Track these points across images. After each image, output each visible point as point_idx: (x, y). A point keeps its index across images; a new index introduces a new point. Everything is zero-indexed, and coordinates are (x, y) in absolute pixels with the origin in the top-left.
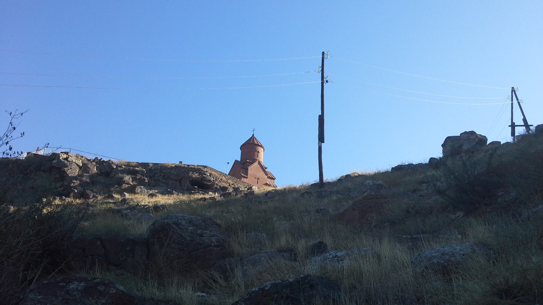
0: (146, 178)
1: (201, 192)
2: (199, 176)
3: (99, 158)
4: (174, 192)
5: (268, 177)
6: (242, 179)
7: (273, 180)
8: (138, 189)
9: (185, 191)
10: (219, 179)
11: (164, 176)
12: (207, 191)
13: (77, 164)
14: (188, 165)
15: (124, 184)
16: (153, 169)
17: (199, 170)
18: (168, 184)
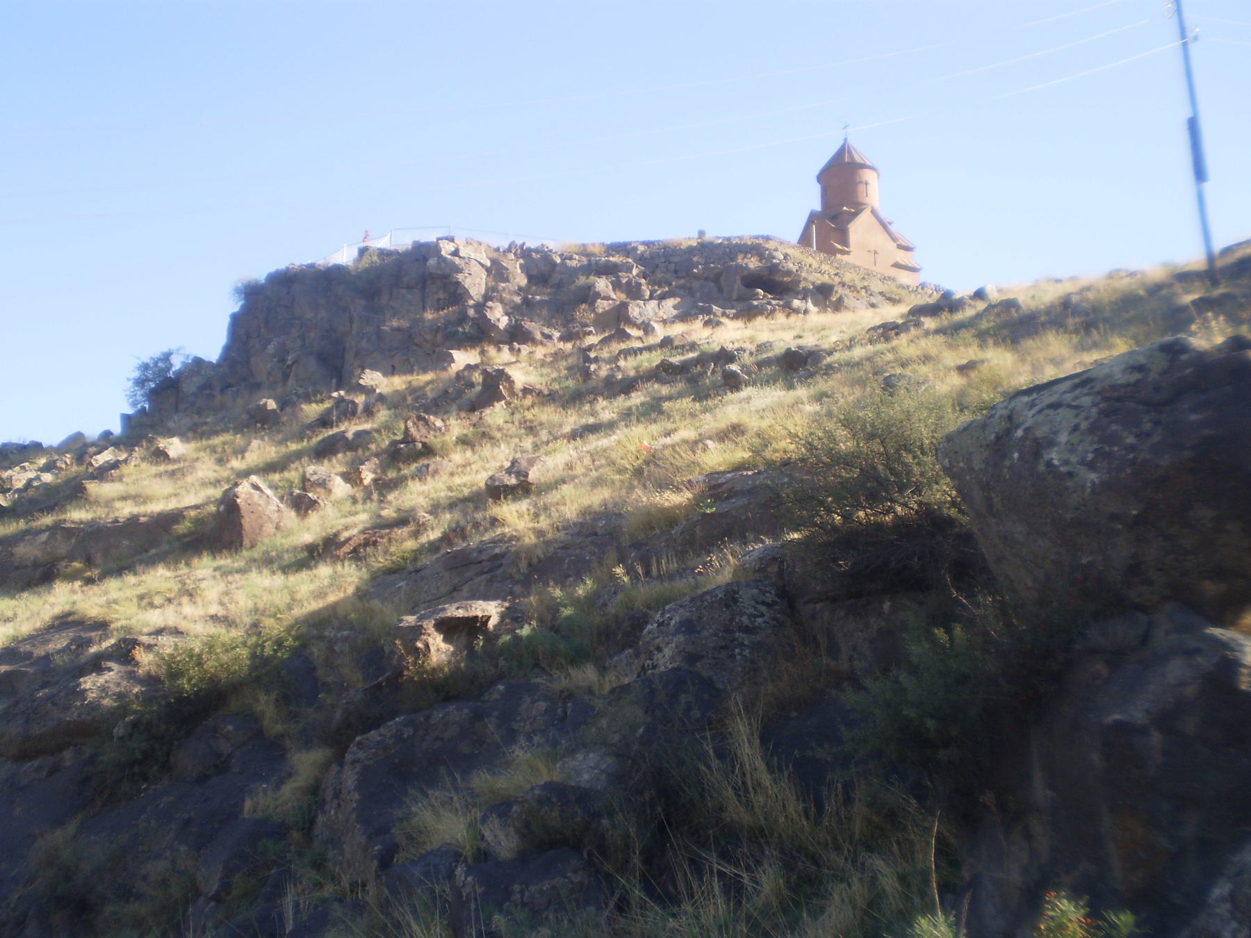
0: (643, 281)
1: (774, 302)
2: (760, 261)
3: (519, 243)
4: (714, 307)
5: (898, 245)
6: (839, 256)
7: (909, 253)
8: (633, 309)
9: (734, 303)
10: (805, 265)
11: (676, 272)
12: (786, 297)
13: (480, 263)
14: (729, 239)
15: (599, 300)
16: (649, 257)
17: (755, 249)
18: (690, 288)
